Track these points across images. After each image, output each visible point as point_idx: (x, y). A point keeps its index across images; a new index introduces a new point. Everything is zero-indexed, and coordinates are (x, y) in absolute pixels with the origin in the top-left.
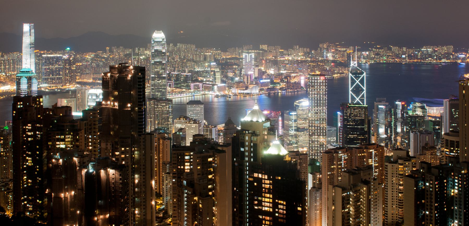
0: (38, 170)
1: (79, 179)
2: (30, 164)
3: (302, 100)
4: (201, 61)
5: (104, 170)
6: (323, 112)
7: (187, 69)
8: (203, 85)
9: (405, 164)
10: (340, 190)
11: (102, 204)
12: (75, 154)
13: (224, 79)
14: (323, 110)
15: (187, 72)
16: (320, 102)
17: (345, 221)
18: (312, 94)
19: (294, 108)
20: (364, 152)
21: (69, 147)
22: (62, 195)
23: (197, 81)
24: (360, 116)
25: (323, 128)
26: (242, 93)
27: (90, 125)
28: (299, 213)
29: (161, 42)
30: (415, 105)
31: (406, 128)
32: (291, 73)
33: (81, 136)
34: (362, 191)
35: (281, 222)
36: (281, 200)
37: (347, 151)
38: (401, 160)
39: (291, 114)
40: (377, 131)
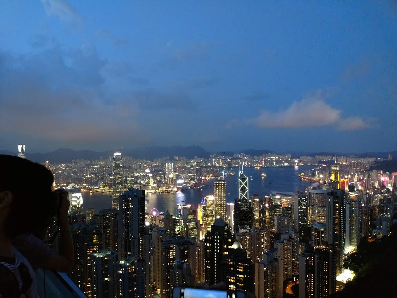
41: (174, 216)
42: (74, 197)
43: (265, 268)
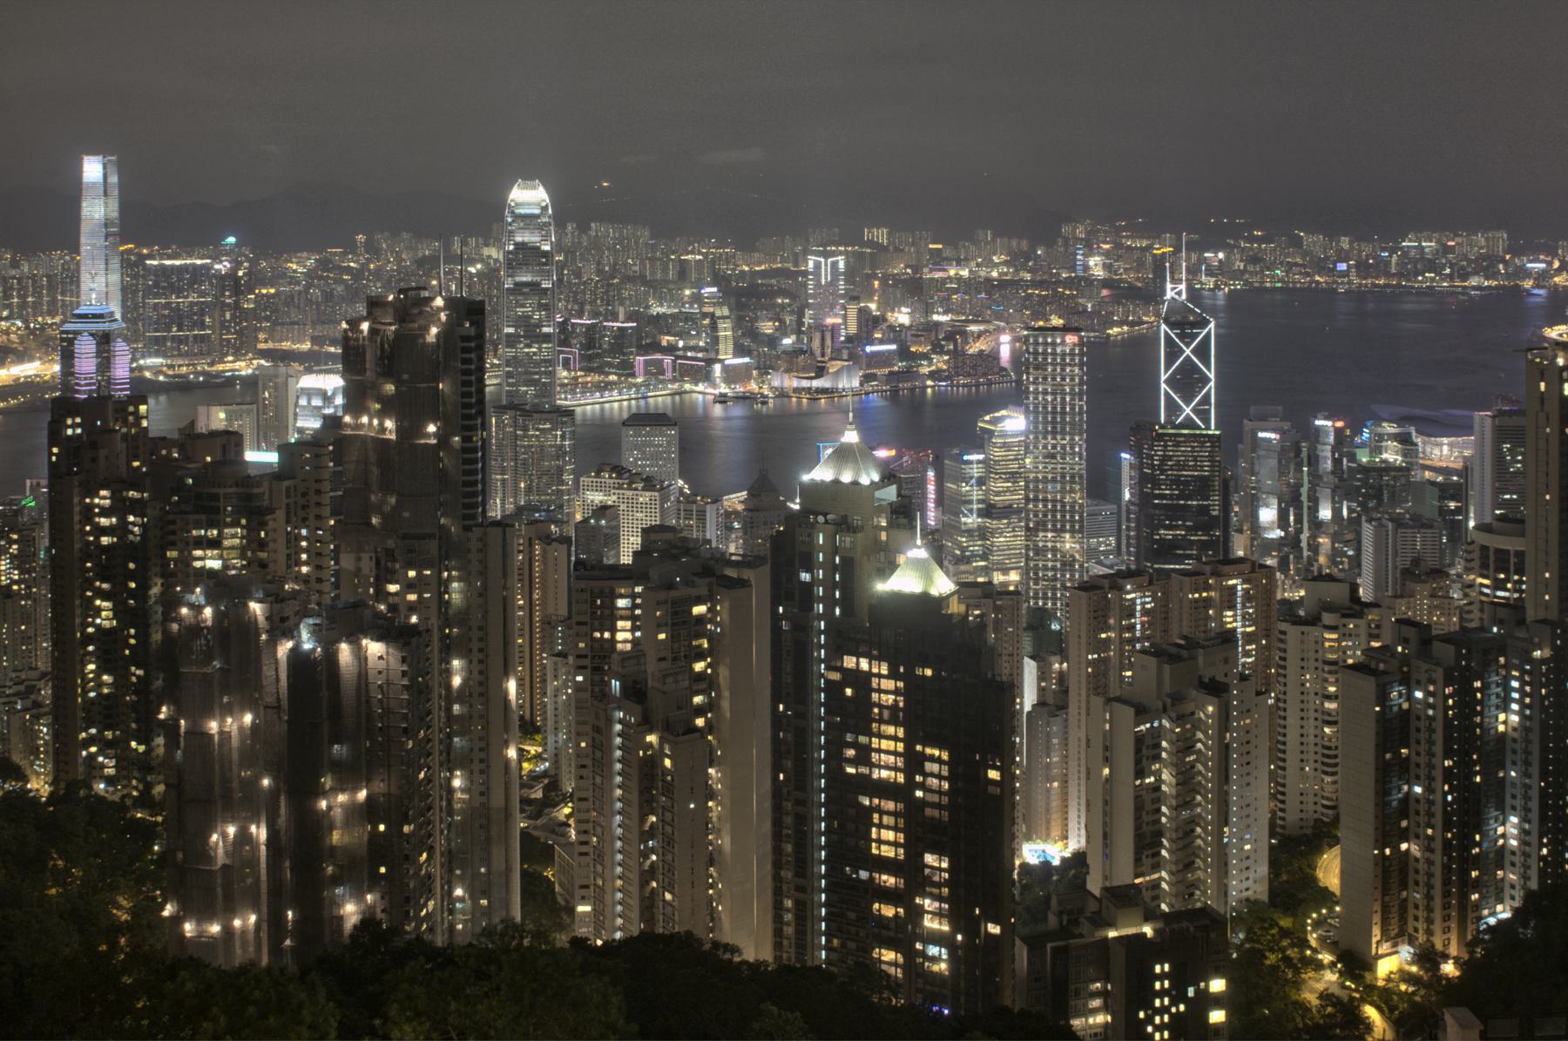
0: (132, 641)
1: (268, 672)
2: (106, 624)
3: (1004, 412)
4: (668, 282)
5: (350, 642)
6: (1074, 454)
7: (621, 310)
8: (674, 361)
9: (1344, 626)
10: (1130, 711)
11: (345, 755)
12: (254, 589)
13: (747, 342)
14: (1072, 448)
15: (621, 317)
16: (1063, 419)
17: (1146, 818)
18: (1036, 392)
19: (980, 441)
20: (1208, 588)
21: (234, 568)
22: (213, 726)
23: (656, 347)
24: (1196, 466)
25: (1072, 507)
26: (803, 389)
27: (304, 495)
28: (992, 790)
29: (537, 216)
30: (1379, 430)
31: (1349, 508)
32: (967, 321)
33: (275, 531)
34: (1202, 715)
35: (933, 818)
36: (933, 746)
37: (1151, 583)
38: (1332, 615)
39: (965, 458)
40: (1255, 516)
42: (309, 393)
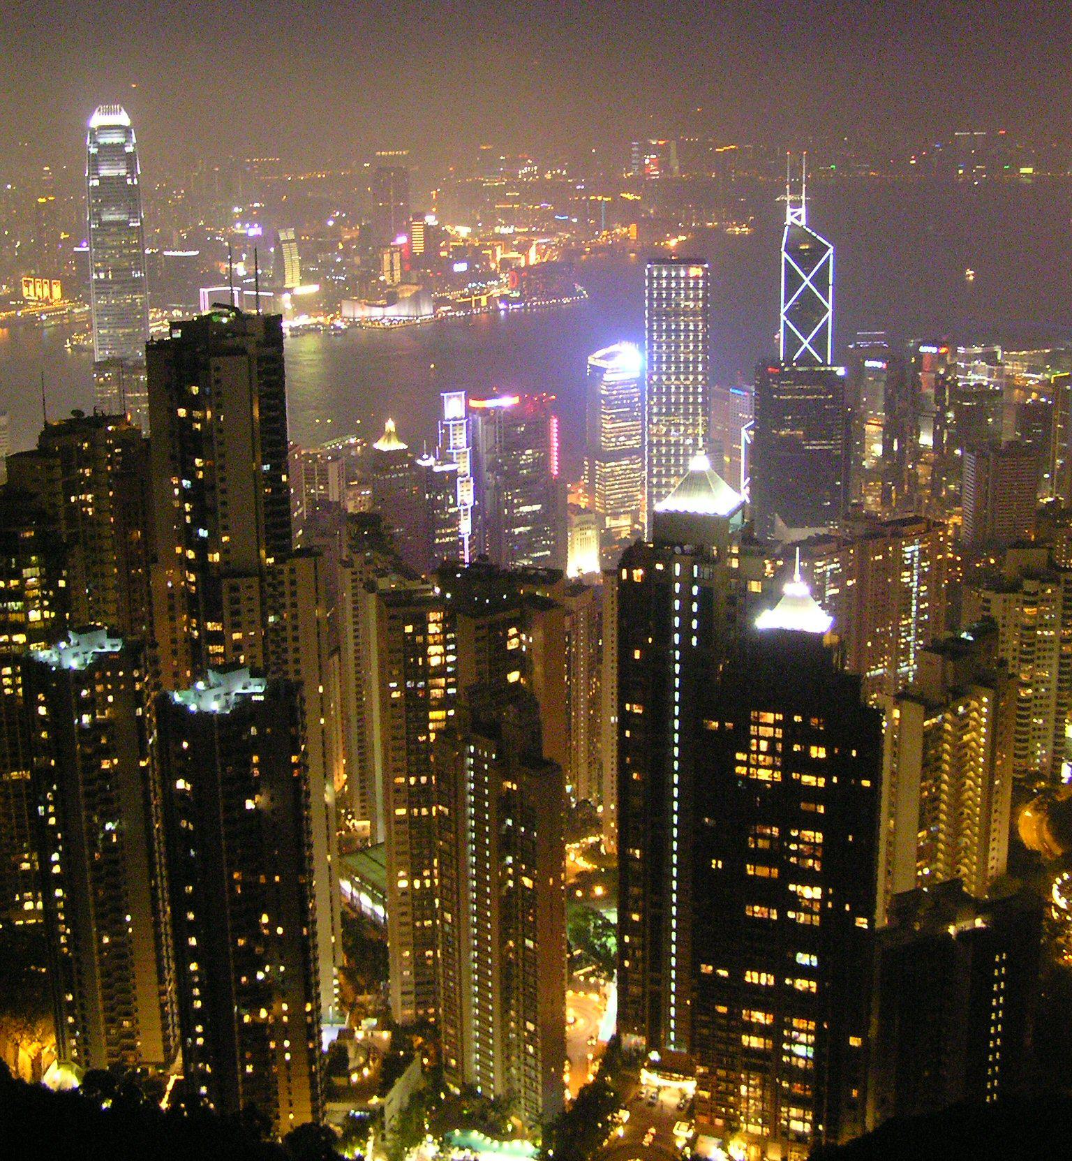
9: (1043, 591)
41: (425, 456)
43: (926, 723)
